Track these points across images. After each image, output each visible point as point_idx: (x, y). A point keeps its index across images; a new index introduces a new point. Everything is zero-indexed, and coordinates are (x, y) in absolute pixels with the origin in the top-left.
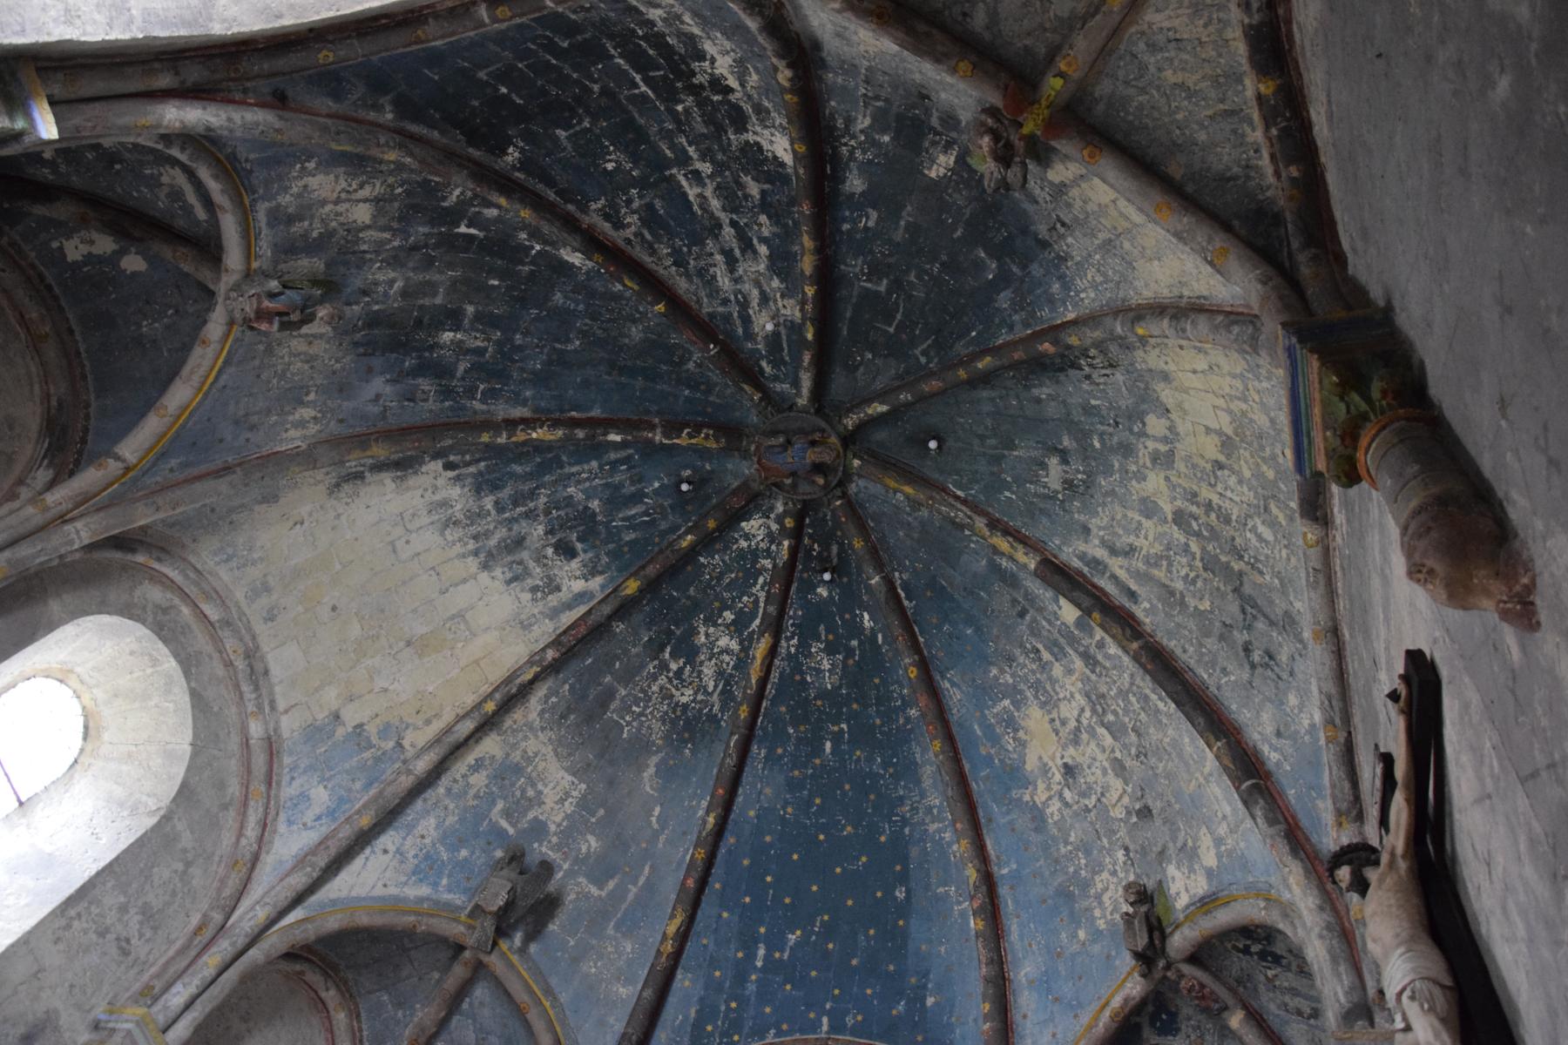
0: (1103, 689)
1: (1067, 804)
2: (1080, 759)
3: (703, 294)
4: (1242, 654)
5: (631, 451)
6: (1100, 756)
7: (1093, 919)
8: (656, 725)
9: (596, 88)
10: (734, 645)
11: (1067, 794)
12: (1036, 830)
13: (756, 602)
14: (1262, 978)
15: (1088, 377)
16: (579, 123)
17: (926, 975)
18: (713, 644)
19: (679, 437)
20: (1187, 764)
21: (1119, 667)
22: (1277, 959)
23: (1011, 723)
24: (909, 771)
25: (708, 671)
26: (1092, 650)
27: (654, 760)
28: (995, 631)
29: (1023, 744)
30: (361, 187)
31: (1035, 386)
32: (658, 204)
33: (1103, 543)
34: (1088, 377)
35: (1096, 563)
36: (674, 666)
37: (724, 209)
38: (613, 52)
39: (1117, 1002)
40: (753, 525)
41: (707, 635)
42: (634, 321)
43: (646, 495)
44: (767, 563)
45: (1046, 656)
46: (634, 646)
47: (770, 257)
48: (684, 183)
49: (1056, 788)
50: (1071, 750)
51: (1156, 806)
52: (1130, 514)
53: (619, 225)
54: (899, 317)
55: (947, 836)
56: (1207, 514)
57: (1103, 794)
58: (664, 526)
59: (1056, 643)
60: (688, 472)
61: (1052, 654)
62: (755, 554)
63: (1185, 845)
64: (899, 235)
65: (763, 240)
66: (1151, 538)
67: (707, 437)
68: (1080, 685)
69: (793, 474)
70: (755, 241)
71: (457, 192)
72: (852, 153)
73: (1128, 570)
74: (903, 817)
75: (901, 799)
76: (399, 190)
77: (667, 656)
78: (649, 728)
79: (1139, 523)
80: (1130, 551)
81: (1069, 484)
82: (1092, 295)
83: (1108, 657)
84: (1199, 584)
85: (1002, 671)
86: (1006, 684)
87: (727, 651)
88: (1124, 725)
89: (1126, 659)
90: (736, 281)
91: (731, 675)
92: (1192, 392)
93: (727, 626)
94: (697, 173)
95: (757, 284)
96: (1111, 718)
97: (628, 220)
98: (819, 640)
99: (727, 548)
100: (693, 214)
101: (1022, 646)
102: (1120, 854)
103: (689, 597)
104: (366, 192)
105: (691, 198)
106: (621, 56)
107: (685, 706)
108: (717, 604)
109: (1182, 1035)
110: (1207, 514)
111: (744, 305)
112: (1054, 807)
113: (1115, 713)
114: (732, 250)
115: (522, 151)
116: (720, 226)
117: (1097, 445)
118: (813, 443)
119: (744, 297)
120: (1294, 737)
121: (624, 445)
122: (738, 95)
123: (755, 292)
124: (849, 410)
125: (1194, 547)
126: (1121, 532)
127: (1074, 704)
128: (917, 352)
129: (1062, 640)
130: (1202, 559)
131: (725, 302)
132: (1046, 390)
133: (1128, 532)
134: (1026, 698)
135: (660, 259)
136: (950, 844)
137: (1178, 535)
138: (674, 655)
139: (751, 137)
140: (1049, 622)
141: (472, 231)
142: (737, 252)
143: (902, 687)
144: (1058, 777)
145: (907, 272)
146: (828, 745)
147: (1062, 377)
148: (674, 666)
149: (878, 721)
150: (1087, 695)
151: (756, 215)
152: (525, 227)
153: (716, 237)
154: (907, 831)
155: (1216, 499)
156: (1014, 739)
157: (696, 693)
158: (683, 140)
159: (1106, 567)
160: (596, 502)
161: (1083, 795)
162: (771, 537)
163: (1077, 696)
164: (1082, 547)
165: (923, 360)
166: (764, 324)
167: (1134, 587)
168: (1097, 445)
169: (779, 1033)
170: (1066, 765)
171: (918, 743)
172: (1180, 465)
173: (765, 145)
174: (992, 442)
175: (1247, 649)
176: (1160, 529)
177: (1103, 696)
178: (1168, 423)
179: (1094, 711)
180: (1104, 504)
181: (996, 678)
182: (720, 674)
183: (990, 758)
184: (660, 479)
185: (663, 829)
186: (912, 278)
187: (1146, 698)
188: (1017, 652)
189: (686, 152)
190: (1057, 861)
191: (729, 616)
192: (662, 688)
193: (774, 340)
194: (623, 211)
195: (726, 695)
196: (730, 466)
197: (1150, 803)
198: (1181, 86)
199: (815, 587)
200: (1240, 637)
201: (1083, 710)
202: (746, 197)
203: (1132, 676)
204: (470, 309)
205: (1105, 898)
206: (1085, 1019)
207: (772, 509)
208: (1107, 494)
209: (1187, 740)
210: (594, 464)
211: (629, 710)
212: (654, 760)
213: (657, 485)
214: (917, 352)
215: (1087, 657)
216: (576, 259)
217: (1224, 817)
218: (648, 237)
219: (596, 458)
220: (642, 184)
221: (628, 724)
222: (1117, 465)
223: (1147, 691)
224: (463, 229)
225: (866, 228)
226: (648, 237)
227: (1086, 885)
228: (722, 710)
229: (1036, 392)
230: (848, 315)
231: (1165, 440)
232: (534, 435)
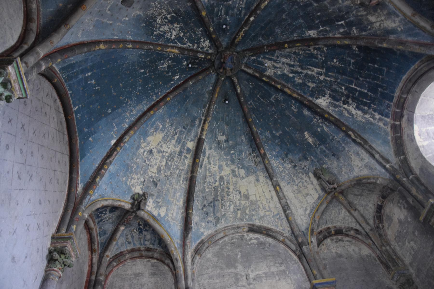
0: (176, 159)
1: (143, 154)
2: (155, 154)
3: (283, 53)
4: (203, 205)
5: (242, 16)
6: (158, 161)
7: (128, 180)
8: (152, 12)
9: (361, 79)
10: (173, 37)
11: (146, 153)
12: (136, 148)
13: (185, 44)
14: (133, 229)
15: (250, 154)
16: (353, 66)
17: (96, 133)
18: (174, 29)
19: (243, 33)
20: (174, 196)
21: (183, 165)
22: (140, 232)
23: (157, 129)
24: (139, 101)
25: (166, 28)
26: (184, 154)
27: (141, 13)
28: (178, 119)
29: (152, 135)
30: (380, 25)
31: (245, 136)
32: (317, 61)
33: (209, 154)
34: (250, 154)
35: (205, 153)
36: (169, 16)
37: (307, 73)
38: (369, 93)
39: (123, 204)
40: (207, 43)
41: (177, 27)
42: (282, 32)
43: (226, 16)
44: (195, 47)
45: (176, 137)
46: (180, 7)
47: (288, 76)
48: (319, 70)
49: (146, 149)
50: (156, 151)
51: (159, 187)
52: (217, 161)
53: (315, 49)
54: (262, 100)
55: (127, 120)
56: (226, 187)
57: (151, 166)
58: (215, 19)
59: (180, 141)
60: (228, 28)
61: (177, 139)
62: (199, 43)
63: (159, 203)
64: (287, 112)
65: (294, 77)
66: (214, 169)
67: (240, 39)
68: (173, 150)
69: (224, 62)
70: (294, 75)
71: (355, 32)
72: (317, 119)
73: (206, 163)
74: (127, 102)
75: (131, 100)
76: (369, 27)
77: (173, 14)
78: (151, 10)
79: (216, 165)
80: (210, 163)
81: (219, 142)
82: (275, 165)
83: (184, 160)
84: (210, 186)
85: (168, 123)
86: (166, 125)
87: (171, 34)
88: (169, 169)
89: (186, 167)
90: (283, 63)
91: (165, 37)
92: (256, 188)
93: (179, 34)
94: (321, 75)
95: (280, 68)
96: (170, 163)
97: (315, 51)
98: (172, 63)
99: (202, 35)
100: (309, 65)
101: (176, 128)
102: (142, 179)
103: (190, 23)
104: (378, 24)
105: (314, 68)
106: (366, 93)
107: (156, 21)
108: (186, 31)
109: (110, 214)
110: (226, 187)
111: (275, 61)
112: (141, 151)
113: (171, 165)
114: (293, 67)
115: (354, 50)
116: (302, 69)
117: (232, 152)
118: (231, 70)
119: (277, 63)
120: (198, 229)
121: (248, 19)
122: (342, 104)
123: (278, 66)
124: (237, 78)
125: (217, 183)
126: (213, 159)
127: (167, 149)
128: (251, 101)
129: (182, 143)
130: (215, 186)
131: (278, 57)
132: (244, 139)
133: (213, 161)
134: (164, 132)
135: (299, 50)
136: (126, 122)
137: (218, 178)
138: (172, 17)
139: (327, 96)
140: (185, 138)
141: (340, 23)
142: (293, 68)
143: (161, 92)
144: (148, 148)
145: (275, 108)
146: (143, 71)
147: (249, 146)
148: (169, 16)
149: (150, 85)
150: (171, 154)
151: (302, 80)
152: (330, 31)
153: (299, 66)
154: (124, 105)
155: (231, 190)
156: (153, 132)
157: (159, 24)
158: (333, 79)
159: (205, 156)
160: (231, 3)
161: (148, 159)
162: (203, 48)
163: (169, 150)
164: (207, 148)
165: (249, 103)
166: (268, 64)
167: (203, 166)
168: (232, 152)
169: (71, 94)
170: (152, 150)
171: (147, 101)
172: (235, 179)
173: (323, 98)
174: (227, 119)
175: (205, 206)
176: (217, 172)
177: (174, 160)
178: (244, 176)
179: (168, 157)
180: (217, 153)
181: (166, 122)
182: (165, 32)
183: (147, 126)
184: (230, 20)
185: (122, 23)
186: (273, 109)
187: (180, 176)
188: (174, 127)
189: (329, 77)
190: (133, 159)
191: (182, 35)
192: (163, 13)
193: (262, 64)
194: (319, 53)
195: (159, 36)
196: (226, 39)
197: (158, 185)
198: (332, 213)
199: (186, 60)
200: (206, 203)
201: (167, 153)
202: (309, 82)
203: (183, 170)
204: (315, 5)
205: (133, 180)
206: (115, 197)
207: (210, 49)
208: (220, 155)
209: (179, 194)
210: (243, 6)
211: (159, 4)
212: (141, 13)
213: (228, 19)
214: (251, 101)
215: (181, 153)
216: (312, 33)
217: (172, 214)
218: (307, 52)
219: (245, 8)
220: (324, 62)
221: (155, 4)
222: (228, 157)
223: (182, 176)
224: (343, 22)
225: (292, 106)
226: (307, 52)
227: (131, 172)
228: (156, 36)
229: (243, 136)
230: (265, 87)
231: (240, 175)
232: (266, 2)
